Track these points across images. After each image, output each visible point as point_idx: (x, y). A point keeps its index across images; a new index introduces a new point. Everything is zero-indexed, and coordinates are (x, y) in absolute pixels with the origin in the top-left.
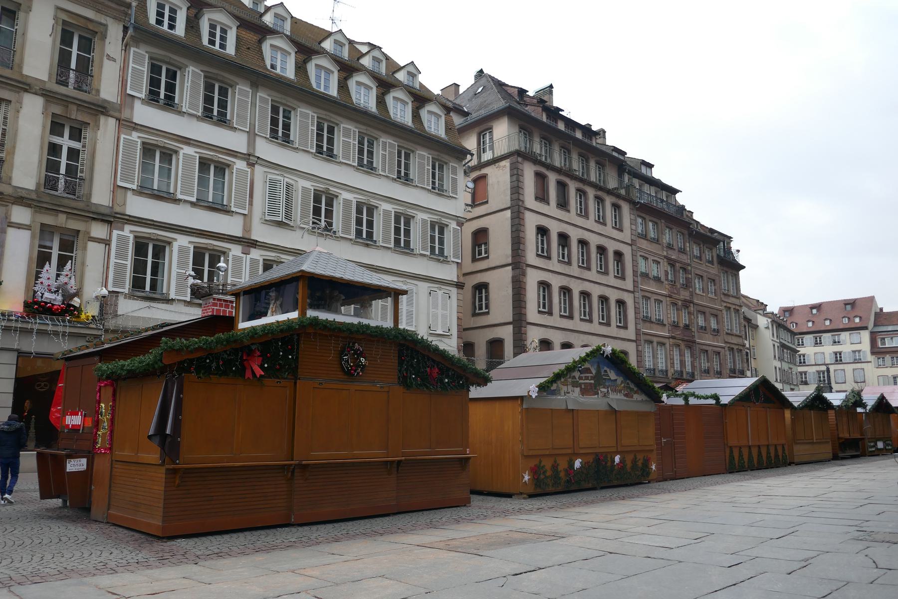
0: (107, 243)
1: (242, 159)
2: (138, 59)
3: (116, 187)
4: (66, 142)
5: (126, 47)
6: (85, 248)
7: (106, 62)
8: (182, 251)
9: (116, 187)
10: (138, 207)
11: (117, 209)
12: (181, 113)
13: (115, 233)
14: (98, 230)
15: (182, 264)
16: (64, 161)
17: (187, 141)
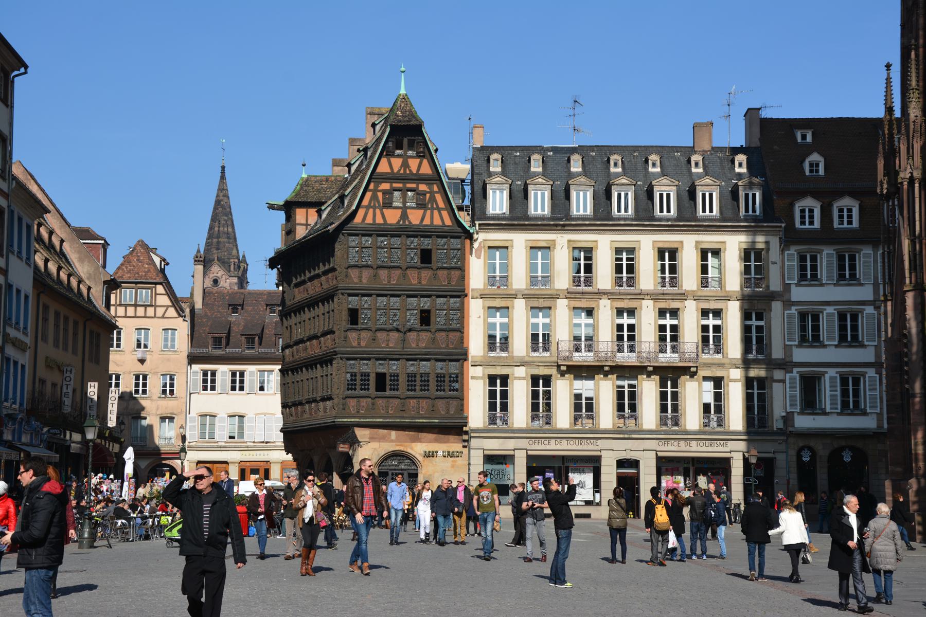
0: (783, 381)
1: (871, 305)
2: (790, 257)
3: (786, 346)
4: (754, 323)
5: (782, 251)
6: (771, 387)
7: (771, 267)
8: (832, 379)
9: (786, 346)
10: (802, 355)
11: (788, 359)
12: (822, 285)
13: (788, 375)
14: (778, 374)
15: (833, 388)
16: (754, 335)
17: (828, 303)
